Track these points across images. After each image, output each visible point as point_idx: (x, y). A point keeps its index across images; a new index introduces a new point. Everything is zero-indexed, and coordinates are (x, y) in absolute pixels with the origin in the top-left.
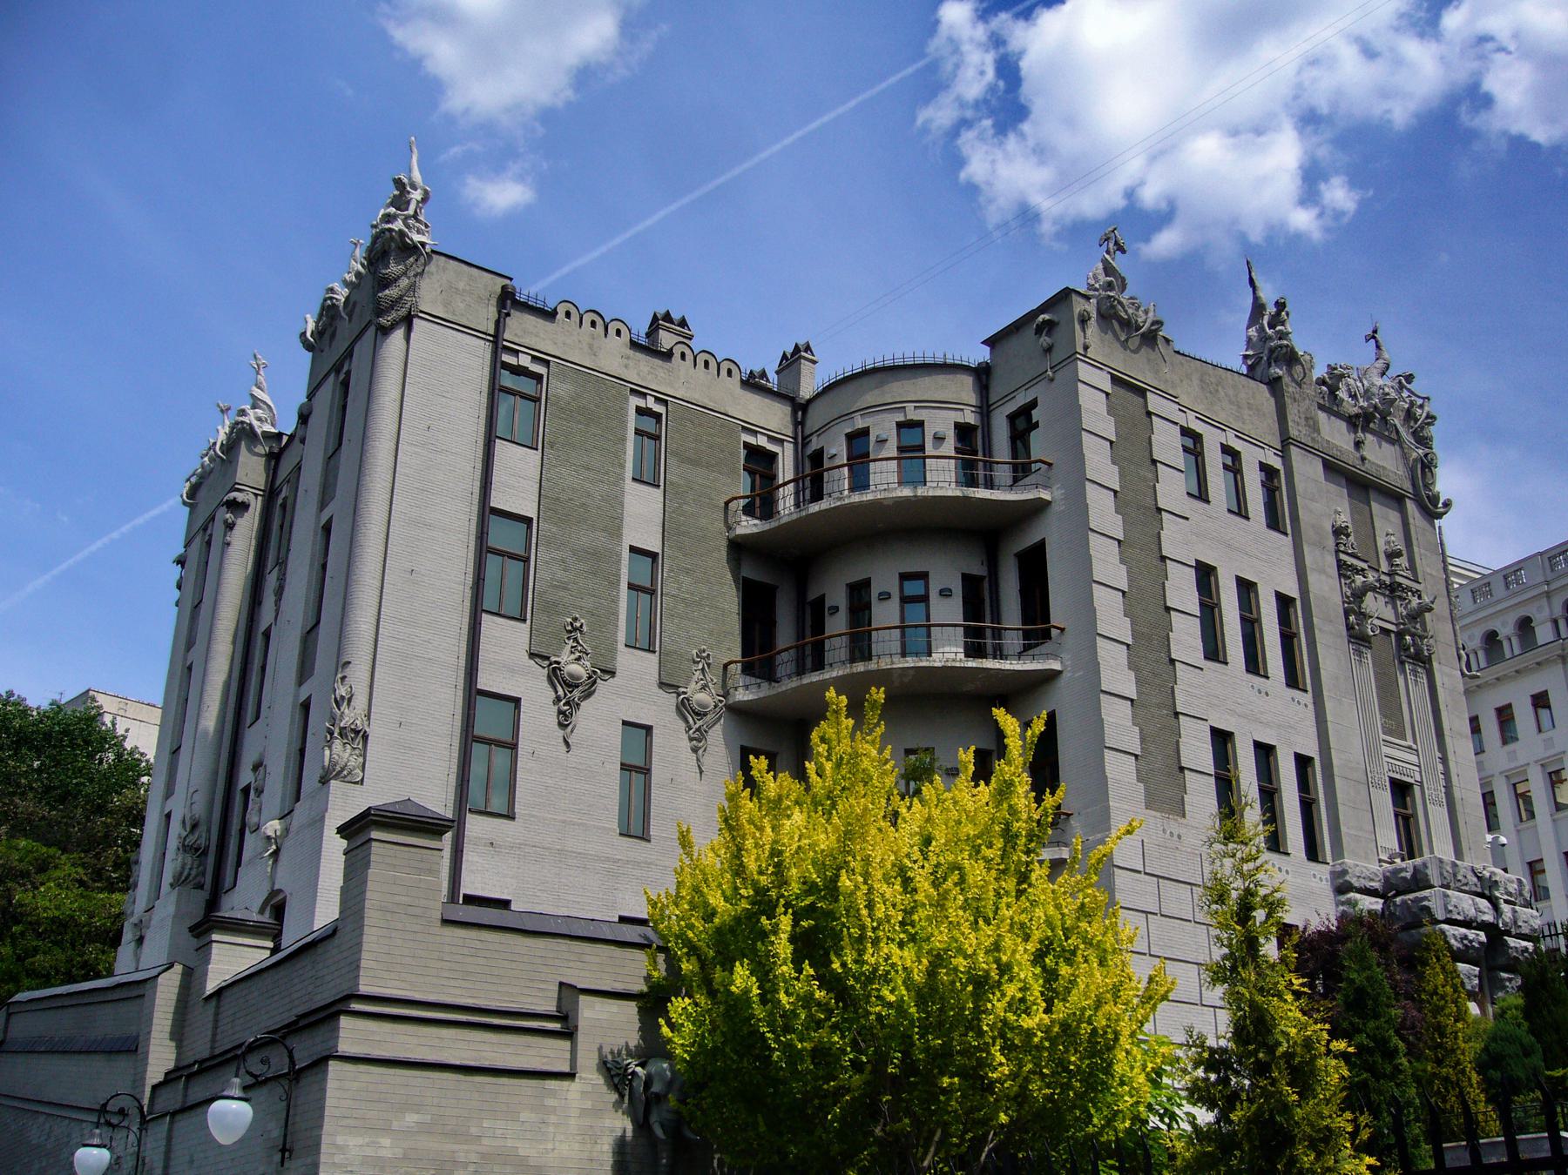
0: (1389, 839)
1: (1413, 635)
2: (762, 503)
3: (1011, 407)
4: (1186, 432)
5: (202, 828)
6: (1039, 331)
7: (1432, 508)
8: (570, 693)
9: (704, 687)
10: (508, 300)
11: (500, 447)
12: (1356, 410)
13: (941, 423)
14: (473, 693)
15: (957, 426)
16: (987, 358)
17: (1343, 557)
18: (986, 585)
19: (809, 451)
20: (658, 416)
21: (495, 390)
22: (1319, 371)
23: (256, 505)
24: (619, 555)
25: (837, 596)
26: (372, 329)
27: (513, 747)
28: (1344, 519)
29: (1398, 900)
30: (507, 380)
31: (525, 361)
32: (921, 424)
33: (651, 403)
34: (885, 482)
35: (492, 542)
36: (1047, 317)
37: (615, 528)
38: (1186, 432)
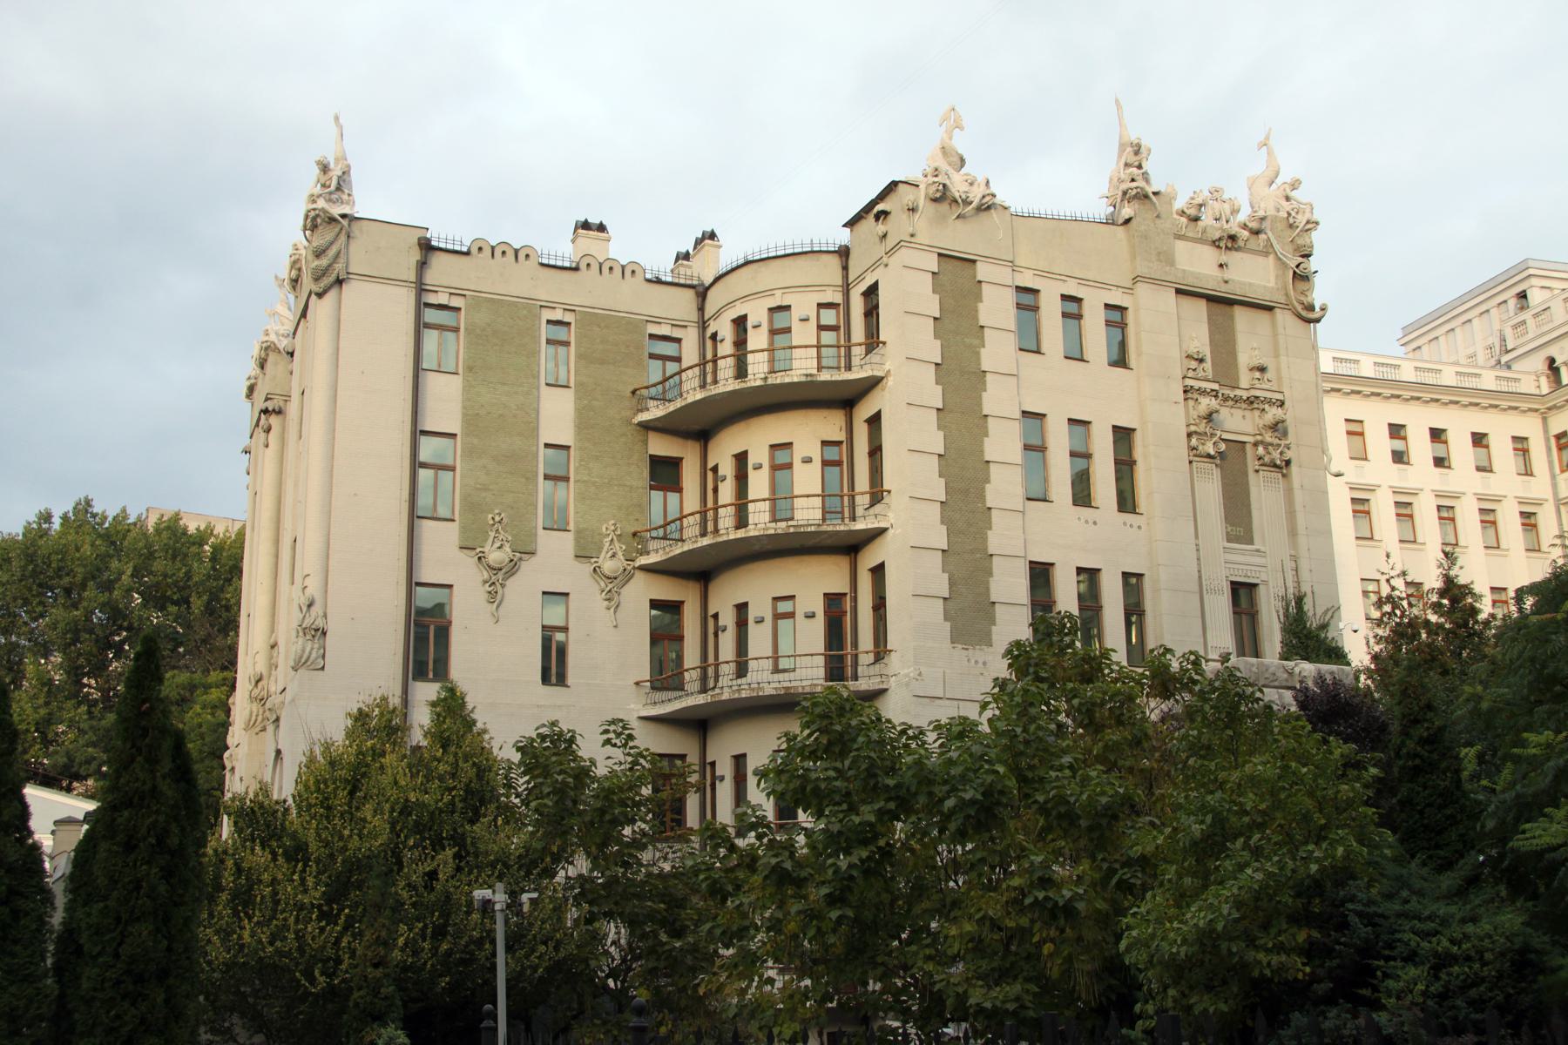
3: (863, 287)
4: (1019, 289)
6: (877, 217)
7: (1309, 316)
10: (427, 247)
12: (1217, 236)
13: (802, 305)
14: (412, 584)
17: (1190, 382)
19: (709, 334)
21: (420, 326)
22: (1179, 204)
30: (431, 316)
31: (442, 299)
32: (788, 308)
33: (557, 315)
35: (424, 456)
37: (533, 430)
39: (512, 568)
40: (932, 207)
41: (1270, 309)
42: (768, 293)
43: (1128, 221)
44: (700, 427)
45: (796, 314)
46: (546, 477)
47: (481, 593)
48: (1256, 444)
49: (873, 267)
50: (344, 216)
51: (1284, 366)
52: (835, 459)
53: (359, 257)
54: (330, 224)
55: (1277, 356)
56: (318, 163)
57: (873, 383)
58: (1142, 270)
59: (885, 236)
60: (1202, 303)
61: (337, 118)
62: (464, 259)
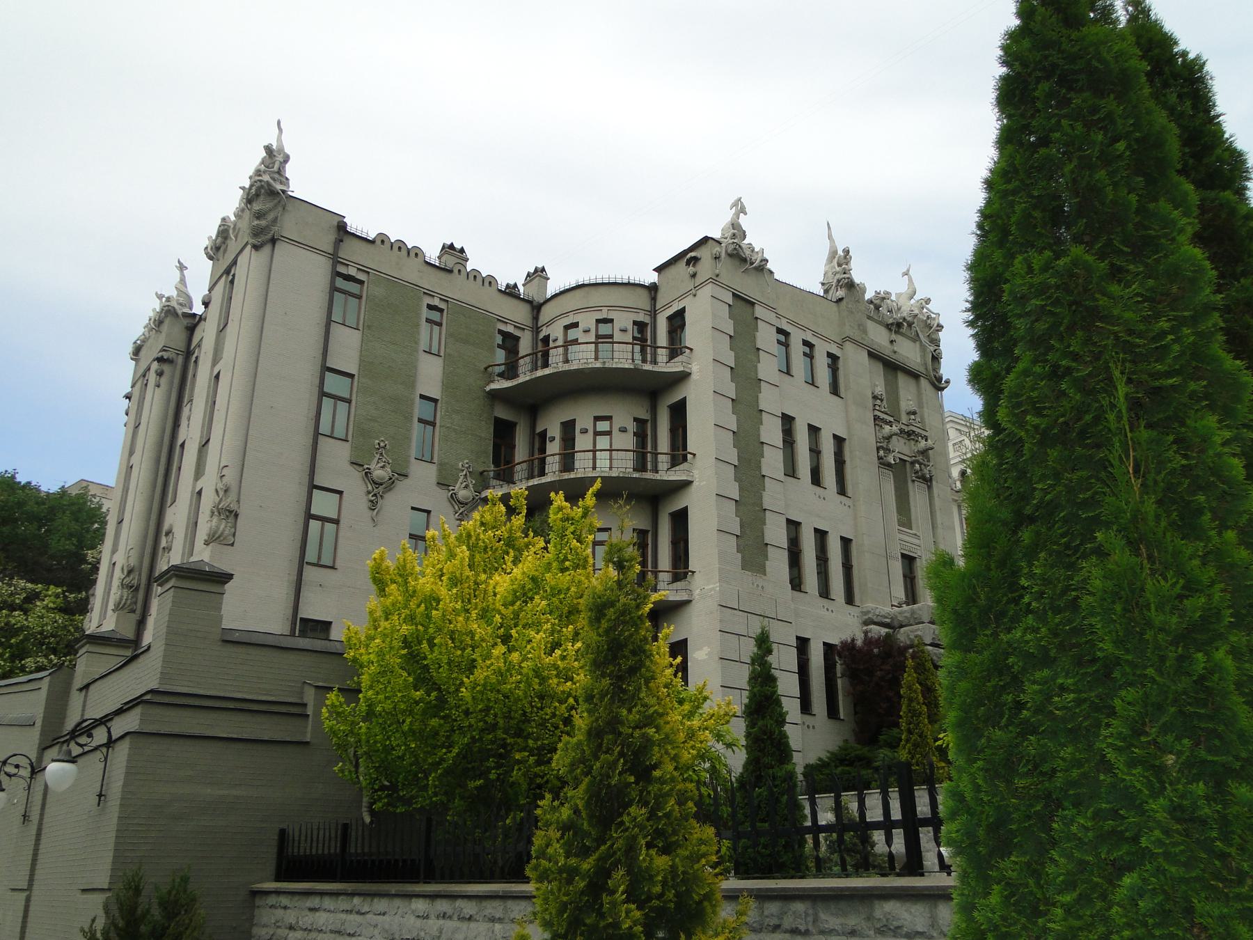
0: (899, 592)
1: (920, 464)
2: (511, 370)
4: (780, 331)
5: (135, 575)
6: (688, 263)
8: (378, 490)
9: (466, 487)
10: (342, 227)
11: (335, 328)
12: (891, 321)
13: (624, 320)
15: (635, 323)
16: (656, 280)
18: (649, 425)
19: (541, 336)
20: (441, 311)
21: (334, 289)
22: (868, 296)
23: (180, 360)
24: (413, 401)
25: (555, 431)
26: (249, 247)
27: (336, 522)
28: (880, 390)
29: (902, 630)
30: (340, 283)
31: (352, 271)
32: (611, 321)
33: (436, 302)
34: (584, 357)
36: (693, 254)
37: (410, 381)
38: (780, 331)
39: (390, 485)
40: (729, 260)
41: (915, 376)
42: (598, 309)
43: (840, 300)
44: (533, 402)
45: (617, 325)
46: (420, 421)
47: (363, 504)
48: (913, 463)
49: (682, 297)
50: (284, 192)
51: (926, 416)
52: (643, 432)
53: (289, 226)
54: (268, 196)
55: (920, 405)
56: (268, 149)
57: (683, 377)
58: (849, 331)
59: (694, 276)
60: (881, 366)
61: (279, 123)
62: (369, 246)
